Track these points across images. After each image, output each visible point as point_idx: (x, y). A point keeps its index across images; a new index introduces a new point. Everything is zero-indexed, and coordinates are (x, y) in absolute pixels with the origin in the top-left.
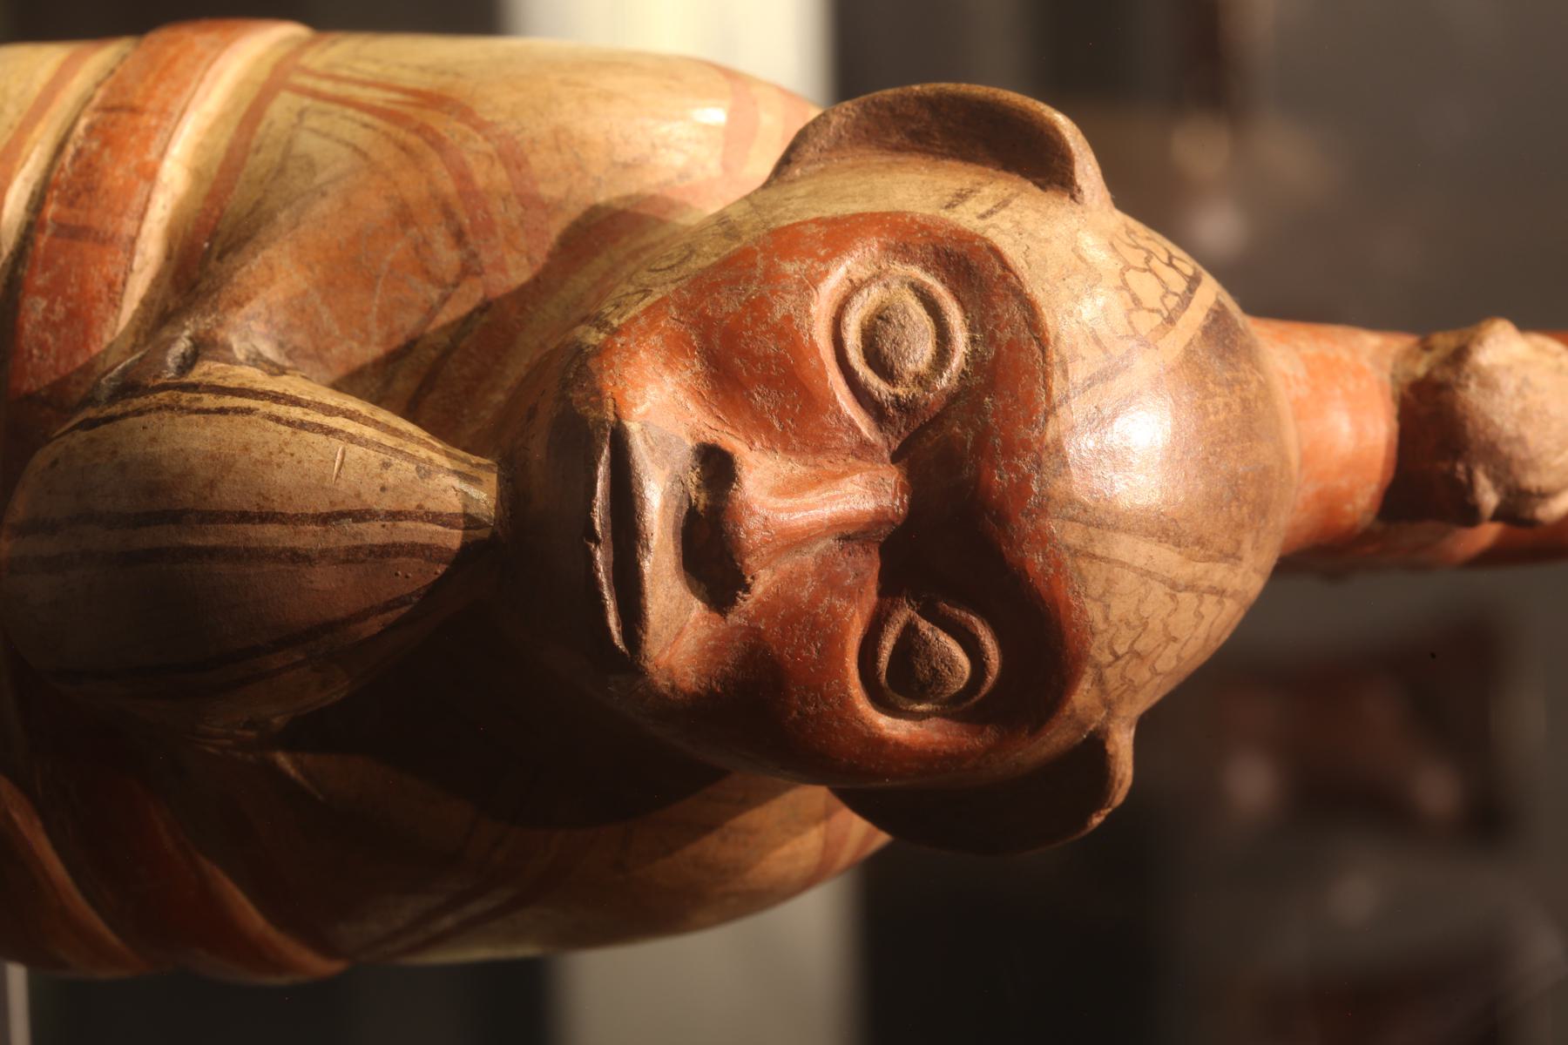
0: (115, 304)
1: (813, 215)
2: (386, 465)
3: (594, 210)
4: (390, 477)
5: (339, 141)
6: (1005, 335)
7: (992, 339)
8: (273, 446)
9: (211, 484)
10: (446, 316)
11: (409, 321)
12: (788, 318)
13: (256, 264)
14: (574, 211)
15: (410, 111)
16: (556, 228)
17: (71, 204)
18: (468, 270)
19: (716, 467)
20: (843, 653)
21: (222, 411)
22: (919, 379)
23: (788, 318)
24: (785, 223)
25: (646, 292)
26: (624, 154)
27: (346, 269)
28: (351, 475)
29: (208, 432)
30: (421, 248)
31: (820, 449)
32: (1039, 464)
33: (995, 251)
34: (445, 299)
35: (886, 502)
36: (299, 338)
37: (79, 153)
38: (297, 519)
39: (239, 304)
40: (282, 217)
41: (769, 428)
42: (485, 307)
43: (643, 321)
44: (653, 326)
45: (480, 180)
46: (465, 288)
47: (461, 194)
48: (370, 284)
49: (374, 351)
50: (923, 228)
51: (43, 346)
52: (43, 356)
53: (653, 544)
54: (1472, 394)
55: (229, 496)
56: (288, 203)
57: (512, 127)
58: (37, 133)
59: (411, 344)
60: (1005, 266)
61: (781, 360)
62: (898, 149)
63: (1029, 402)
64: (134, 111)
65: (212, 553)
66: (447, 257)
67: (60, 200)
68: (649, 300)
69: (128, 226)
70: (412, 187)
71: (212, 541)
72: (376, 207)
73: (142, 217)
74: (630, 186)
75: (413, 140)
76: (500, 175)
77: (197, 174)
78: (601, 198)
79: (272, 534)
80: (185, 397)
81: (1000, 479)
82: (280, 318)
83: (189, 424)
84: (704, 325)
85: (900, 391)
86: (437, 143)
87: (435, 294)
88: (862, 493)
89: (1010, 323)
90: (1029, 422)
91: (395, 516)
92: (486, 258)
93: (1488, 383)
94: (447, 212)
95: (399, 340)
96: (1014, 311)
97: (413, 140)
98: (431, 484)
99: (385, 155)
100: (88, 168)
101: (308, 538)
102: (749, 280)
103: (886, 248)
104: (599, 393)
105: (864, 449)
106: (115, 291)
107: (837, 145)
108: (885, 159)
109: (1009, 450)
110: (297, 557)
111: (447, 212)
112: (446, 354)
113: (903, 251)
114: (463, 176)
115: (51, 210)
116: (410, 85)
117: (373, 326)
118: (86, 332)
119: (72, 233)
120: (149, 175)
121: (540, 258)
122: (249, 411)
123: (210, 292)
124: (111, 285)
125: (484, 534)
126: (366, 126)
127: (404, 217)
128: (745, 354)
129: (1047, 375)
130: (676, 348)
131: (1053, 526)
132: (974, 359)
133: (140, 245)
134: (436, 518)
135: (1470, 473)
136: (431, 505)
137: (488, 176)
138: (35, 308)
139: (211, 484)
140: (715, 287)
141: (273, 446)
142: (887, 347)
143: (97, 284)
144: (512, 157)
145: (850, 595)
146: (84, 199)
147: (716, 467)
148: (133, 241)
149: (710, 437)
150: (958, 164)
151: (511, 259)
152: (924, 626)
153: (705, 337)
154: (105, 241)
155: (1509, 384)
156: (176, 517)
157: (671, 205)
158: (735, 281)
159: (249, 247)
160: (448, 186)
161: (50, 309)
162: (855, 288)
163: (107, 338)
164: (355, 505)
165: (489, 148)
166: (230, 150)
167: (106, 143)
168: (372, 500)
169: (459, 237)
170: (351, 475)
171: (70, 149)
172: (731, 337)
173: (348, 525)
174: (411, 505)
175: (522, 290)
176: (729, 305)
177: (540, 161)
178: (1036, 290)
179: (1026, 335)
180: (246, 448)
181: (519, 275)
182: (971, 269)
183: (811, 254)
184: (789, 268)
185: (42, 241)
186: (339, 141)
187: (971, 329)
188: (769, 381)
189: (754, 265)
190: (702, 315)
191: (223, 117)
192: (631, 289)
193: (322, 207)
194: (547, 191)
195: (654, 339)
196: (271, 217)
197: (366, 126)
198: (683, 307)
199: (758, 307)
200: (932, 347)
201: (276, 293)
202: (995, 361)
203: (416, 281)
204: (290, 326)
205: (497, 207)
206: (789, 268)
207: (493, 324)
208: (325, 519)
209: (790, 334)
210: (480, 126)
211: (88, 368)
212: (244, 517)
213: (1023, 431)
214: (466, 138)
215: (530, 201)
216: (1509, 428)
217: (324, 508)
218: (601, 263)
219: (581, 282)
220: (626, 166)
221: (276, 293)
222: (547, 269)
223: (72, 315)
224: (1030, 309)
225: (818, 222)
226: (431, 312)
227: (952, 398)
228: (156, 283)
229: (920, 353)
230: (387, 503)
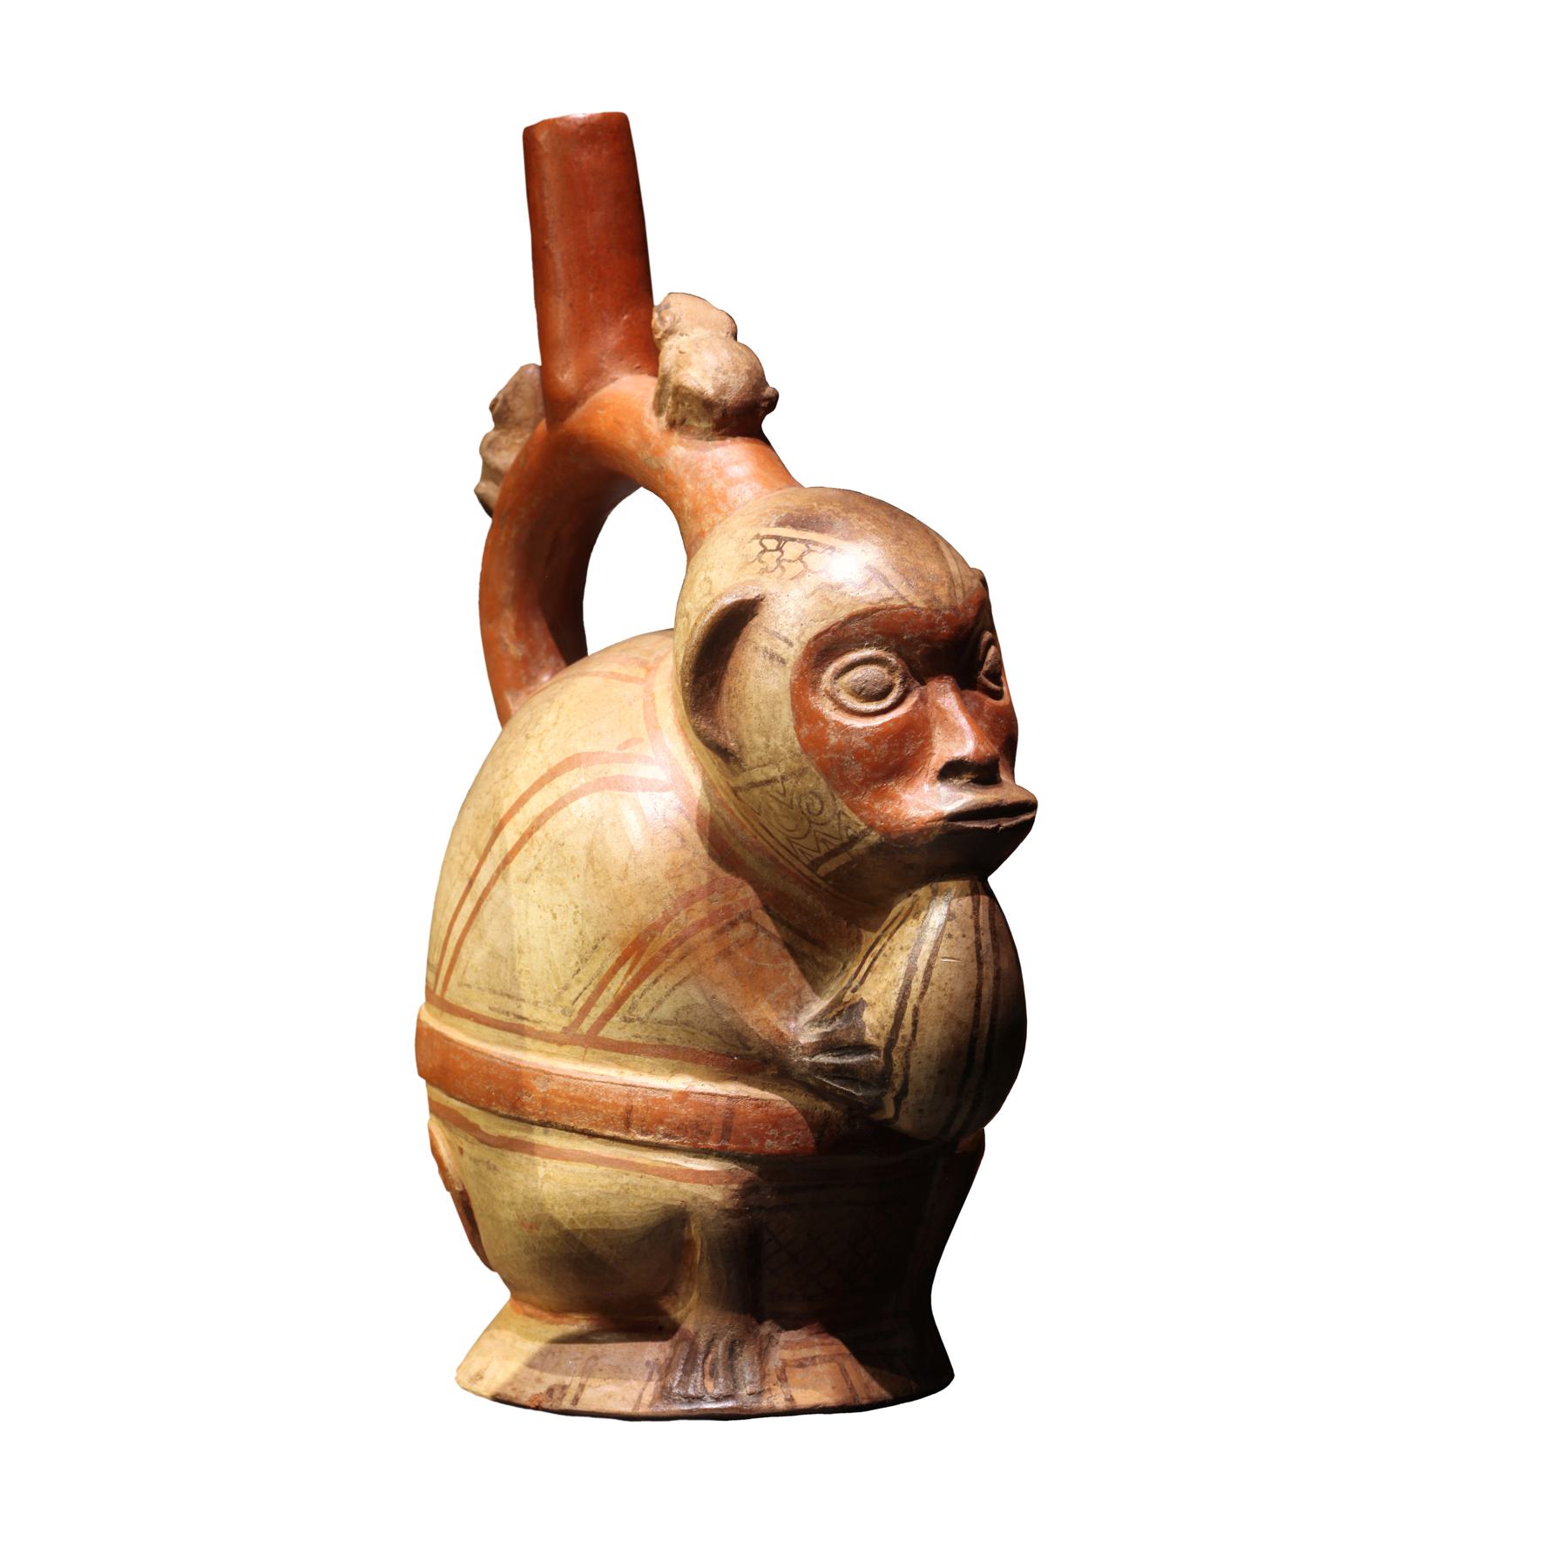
0: (768, 1103)
1: (792, 731)
2: (950, 936)
3: (711, 855)
4: (957, 933)
5: (668, 995)
6: (868, 630)
7: (870, 637)
8: (941, 994)
9: (960, 1023)
10: (773, 930)
11: (776, 947)
12: (867, 739)
13: (756, 1029)
14: (713, 865)
15: (644, 959)
16: (722, 874)
17: (708, 1134)
18: (749, 919)
19: (952, 771)
20: (894, 721)
21: (915, 1023)
22: (891, 672)
23: (867, 739)
24: (797, 745)
25: (842, 813)
26: (676, 842)
27: (754, 982)
28: (957, 953)
29: (929, 1029)
30: (741, 944)
31: (927, 721)
32: (937, 611)
33: (817, 637)
34: (764, 929)
35: (949, 687)
36: (792, 1003)
37: (666, 1136)
38: (980, 977)
39: (782, 1034)
40: (726, 1018)
41: (923, 746)
42: (766, 908)
43: (864, 813)
44: (868, 808)
45: (703, 915)
46: (757, 919)
47: (711, 925)
48: (761, 968)
49: (792, 964)
50: (802, 674)
51: (791, 1139)
52: (801, 1138)
53: (999, 797)
54: (730, 398)
55: (966, 1014)
56: (718, 1015)
57: (668, 902)
58: (640, 1161)
59: (787, 945)
60: (826, 631)
61: (891, 741)
62: (718, 693)
63: (907, 617)
64: (629, 1112)
65: (993, 1020)
66: (744, 929)
67: (705, 1140)
68: (848, 811)
69: (721, 1101)
70: (711, 950)
71: (987, 1021)
72: (722, 968)
73: (715, 1095)
74: (694, 837)
75: (676, 953)
76: (698, 905)
77: (675, 1071)
78: (704, 852)
79: (986, 991)
80: (899, 1044)
81: (945, 630)
82: (784, 1013)
83: (923, 1039)
84: (867, 782)
85: (898, 682)
86: (680, 941)
87: (762, 935)
88: (947, 699)
89: (861, 627)
90: (918, 616)
91: (977, 929)
92: (742, 910)
93: (723, 389)
94: (721, 931)
95: (785, 952)
96: (854, 626)
97: (676, 953)
98: (958, 913)
99: (684, 969)
100: (681, 1128)
101: (989, 972)
102: (841, 760)
103: (814, 693)
104: (921, 831)
105: (923, 699)
106: (759, 1104)
107: (716, 725)
108: (724, 698)
109: (932, 625)
110: (997, 978)
111: (721, 931)
112: (790, 927)
113: (815, 684)
114: (701, 924)
115: (711, 1144)
116: (611, 962)
117: (780, 966)
118: (781, 1116)
119: (727, 1129)
120: (683, 1096)
121: (739, 881)
122: (916, 1010)
123: (774, 1050)
124: (758, 1106)
125: (979, 885)
126: (655, 981)
127: (726, 953)
128: (887, 759)
129: (893, 608)
130: (881, 795)
131: (960, 603)
132: (879, 646)
133: (733, 1094)
134: (976, 909)
135: (765, 399)
136: (970, 912)
137: (700, 911)
138: (771, 1145)
139: (960, 1023)
140: (842, 778)
141: (941, 994)
142: (878, 689)
143: (758, 1114)
144: (689, 899)
145: (982, 704)
146: (704, 1128)
147: (952, 771)
148: (730, 1098)
149: (932, 775)
150: (732, 662)
151: (741, 896)
152: (986, 668)
153: (876, 781)
154: (732, 1112)
155: (722, 379)
156: (973, 1039)
157: (700, 816)
158: (841, 768)
159: (746, 1034)
160: (708, 932)
161: (772, 1137)
162: (841, 707)
163: (788, 1105)
164: (973, 949)
165: (683, 913)
166: (657, 1056)
167: (661, 1122)
168: (970, 941)
169: (733, 924)
170: (957, 953)
171: (665, 1141)
172: (876, 767)
173: (983, 951)
174: (971, 922)
175: (756, 890)
176: (857, 770)
177: (688, 884)
178: (842, 615)
179: (869, 620)
180: (941, 1008)
181: (749, 892)
182: (825, 649)
183: (823, 729)
184: (833, 740)
185: (732, 1146)
186: (668, 995)
187: (861, 647)
188: (901, 747)
189: (831, 759)
190: (862, 783)
191: (620, 1065)
192: (835, 822)
193: (722, 997)
194: (704, 880)
195: (877, 806)
196: (727, 1024)
197: (655, 981)
198: (856, 792)
199: (859, 755)
200: (867, 667)
201: (772, 1016)
202: (882, 633)
203: (757, 945)
204: (787, 1008)
205: (716, 905)
206: (833, 740)
207: (775, 903)
208: (980, 964)
209: (876, 738)
210: (667, 919)
211: (805, 1113)
212: (978, 1005)
213: (922, 619)
214: (677, 925)
215: (710, 889)
216: (745, 378)
217: (975, 965)
218: (738, 850)
219: (750, 859)
220: (683, 840)
221: (772, 1016)
222: (745, 878)
223: (775, 1125)
224: (852, 618)
225: (797, 729)
226: (771, 936)
227: (899, 655)
228: (751, 1084)
229: (872, 671)
230: (971, 933)
